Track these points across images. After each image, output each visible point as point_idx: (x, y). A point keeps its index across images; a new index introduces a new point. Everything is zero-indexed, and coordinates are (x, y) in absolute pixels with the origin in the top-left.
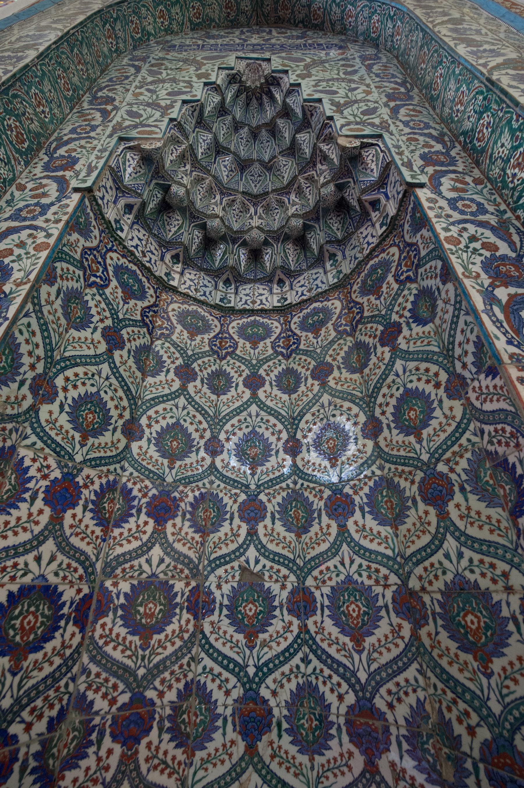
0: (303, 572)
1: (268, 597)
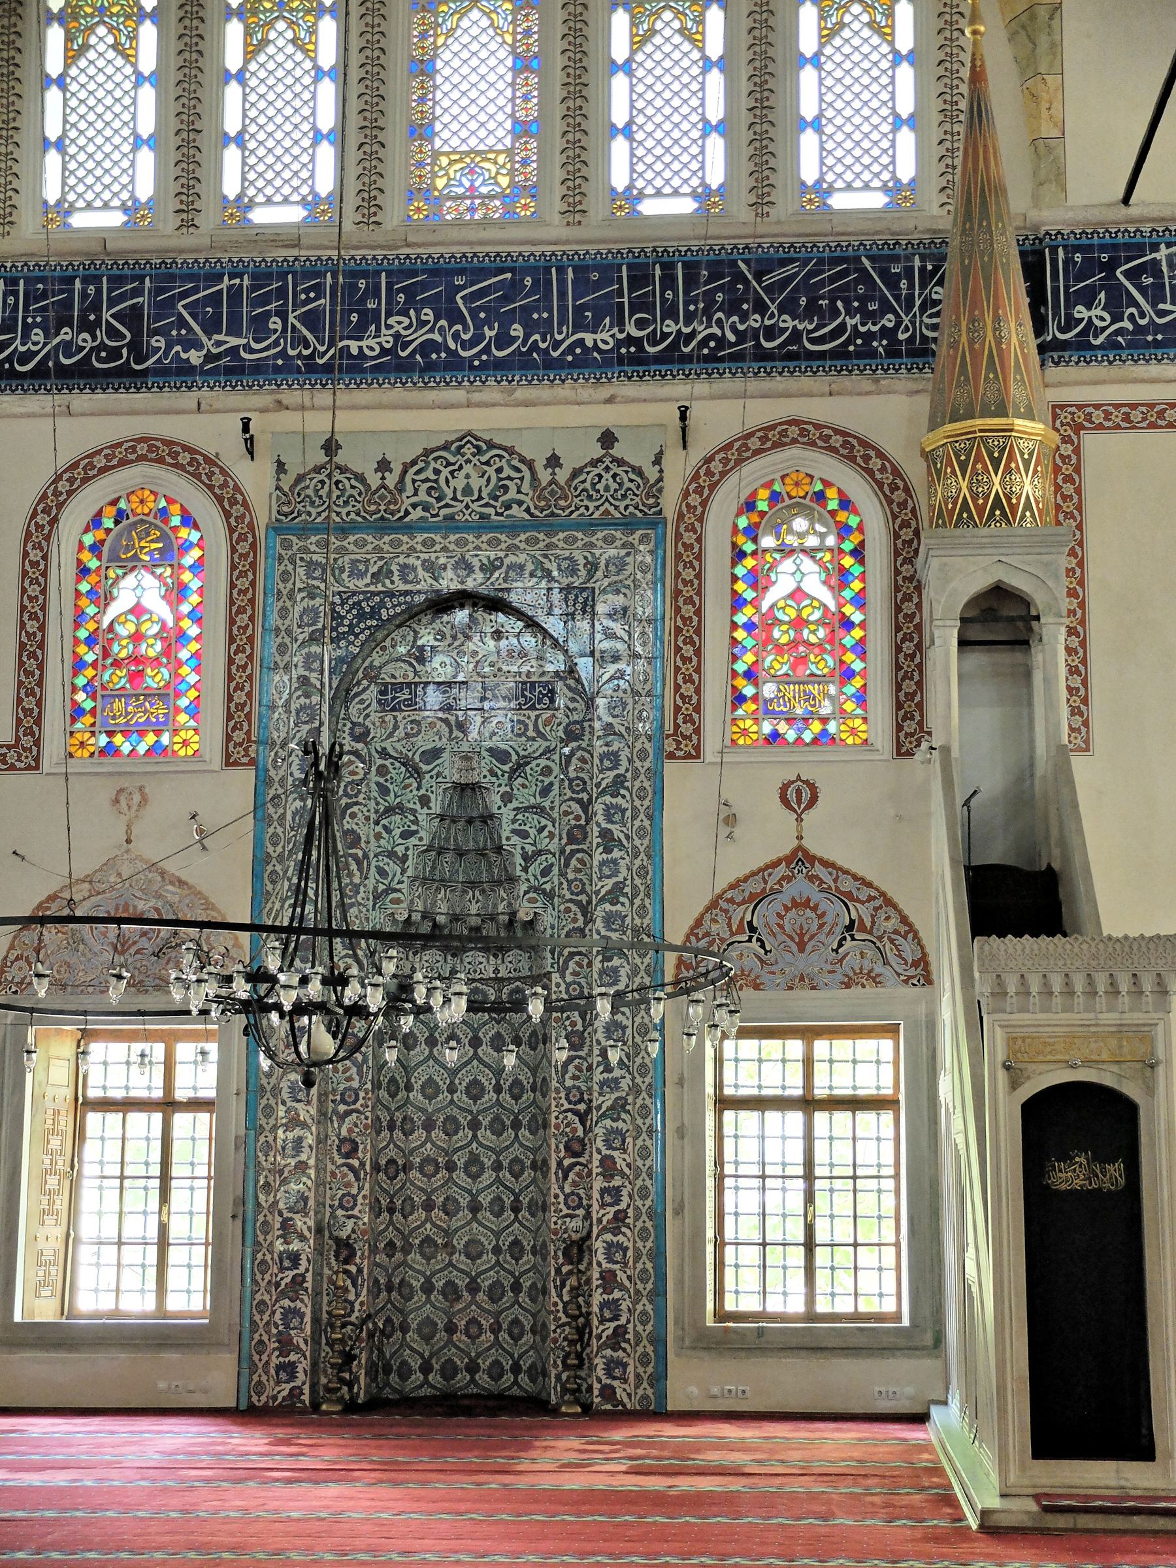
0: (498, 1154)
1: (482, 1164)
